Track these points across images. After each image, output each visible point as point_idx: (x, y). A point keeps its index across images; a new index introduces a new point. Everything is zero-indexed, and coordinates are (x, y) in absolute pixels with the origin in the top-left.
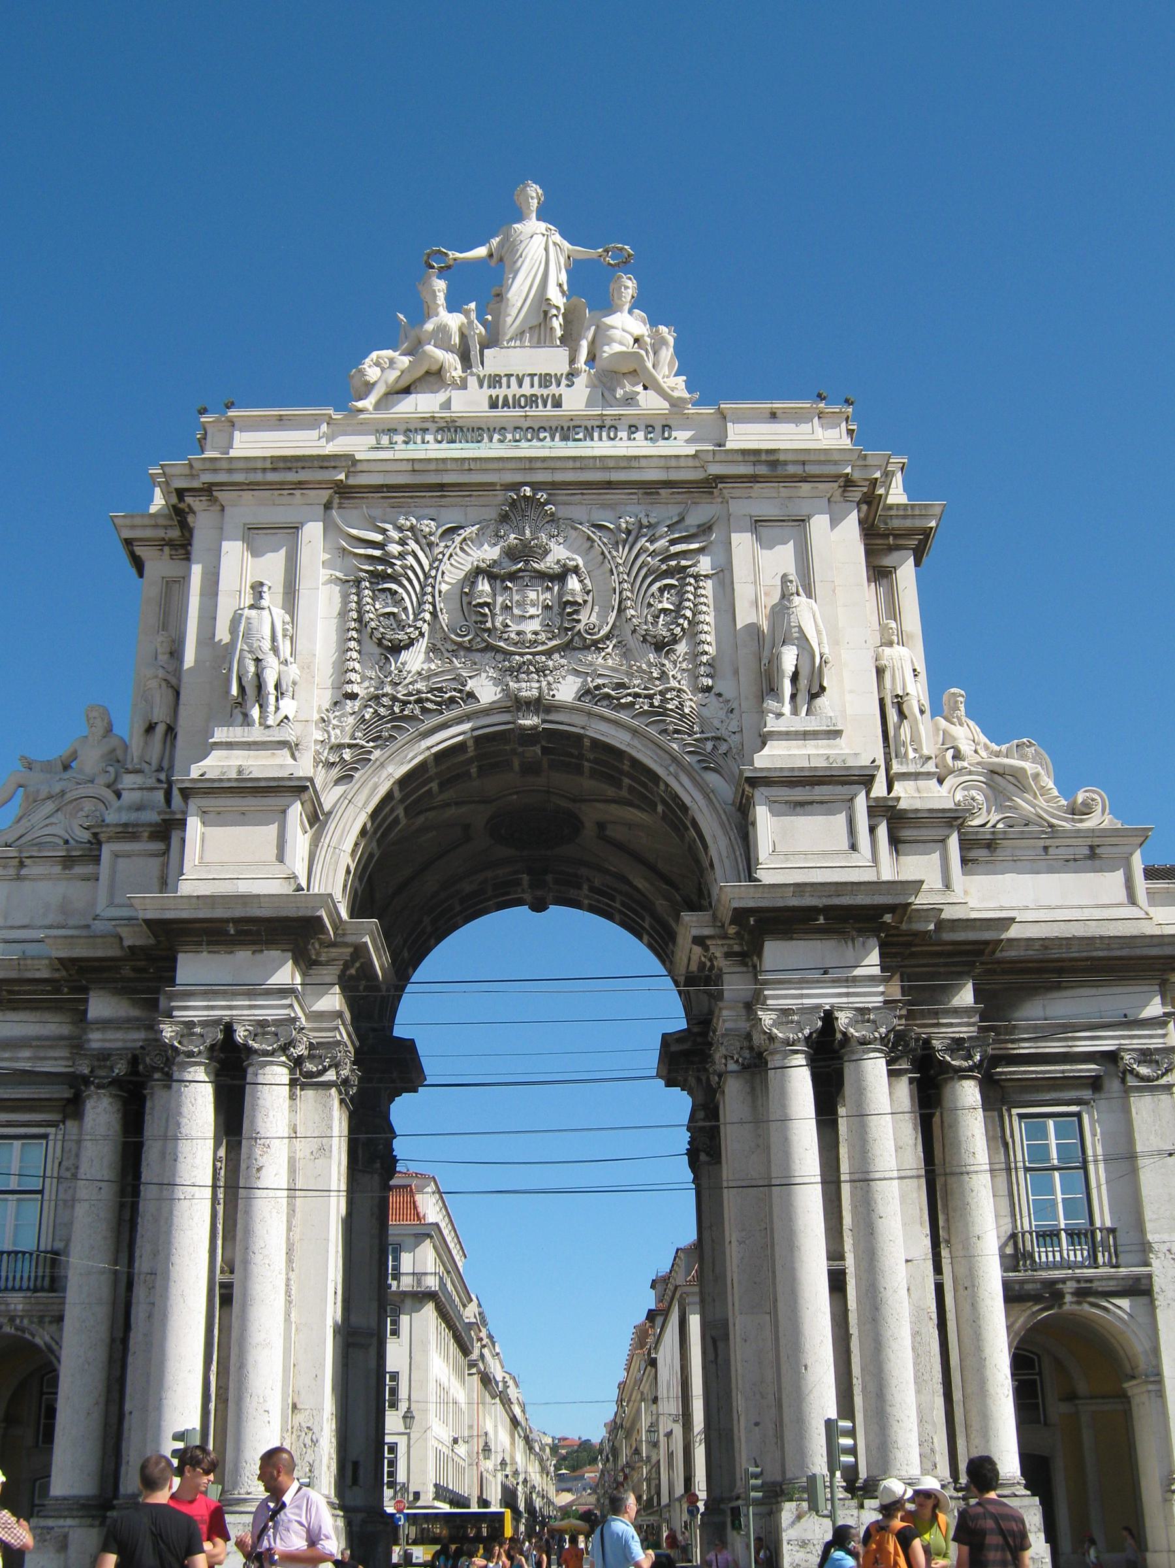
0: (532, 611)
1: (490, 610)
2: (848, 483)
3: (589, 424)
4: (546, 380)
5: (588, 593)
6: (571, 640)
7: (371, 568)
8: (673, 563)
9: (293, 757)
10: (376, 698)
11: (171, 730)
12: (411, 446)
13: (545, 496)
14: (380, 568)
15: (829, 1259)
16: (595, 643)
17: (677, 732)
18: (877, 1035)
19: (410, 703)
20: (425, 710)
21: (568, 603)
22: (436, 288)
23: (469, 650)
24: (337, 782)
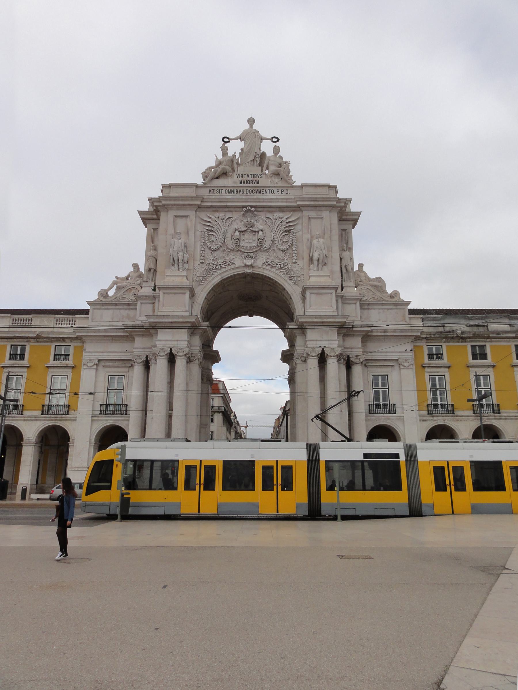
0: (250, 241)
1: (239, 241)
2: (334, 207)
3: (266, 189)
4: (255, 176)
6: (260, 249)
7: (207, 228)
8: (288, 228)
9: (187, 279)
10: (209, 263)
11: (155, 270)
13: (254, 209)
14: (210, 228)
15: (321, 411)
16: (266, 250)
17: (287, 274)
18: (335, 355)
19: (218, 265)
20: (221, 267)
21: (259, 239)
23: (234, 251)
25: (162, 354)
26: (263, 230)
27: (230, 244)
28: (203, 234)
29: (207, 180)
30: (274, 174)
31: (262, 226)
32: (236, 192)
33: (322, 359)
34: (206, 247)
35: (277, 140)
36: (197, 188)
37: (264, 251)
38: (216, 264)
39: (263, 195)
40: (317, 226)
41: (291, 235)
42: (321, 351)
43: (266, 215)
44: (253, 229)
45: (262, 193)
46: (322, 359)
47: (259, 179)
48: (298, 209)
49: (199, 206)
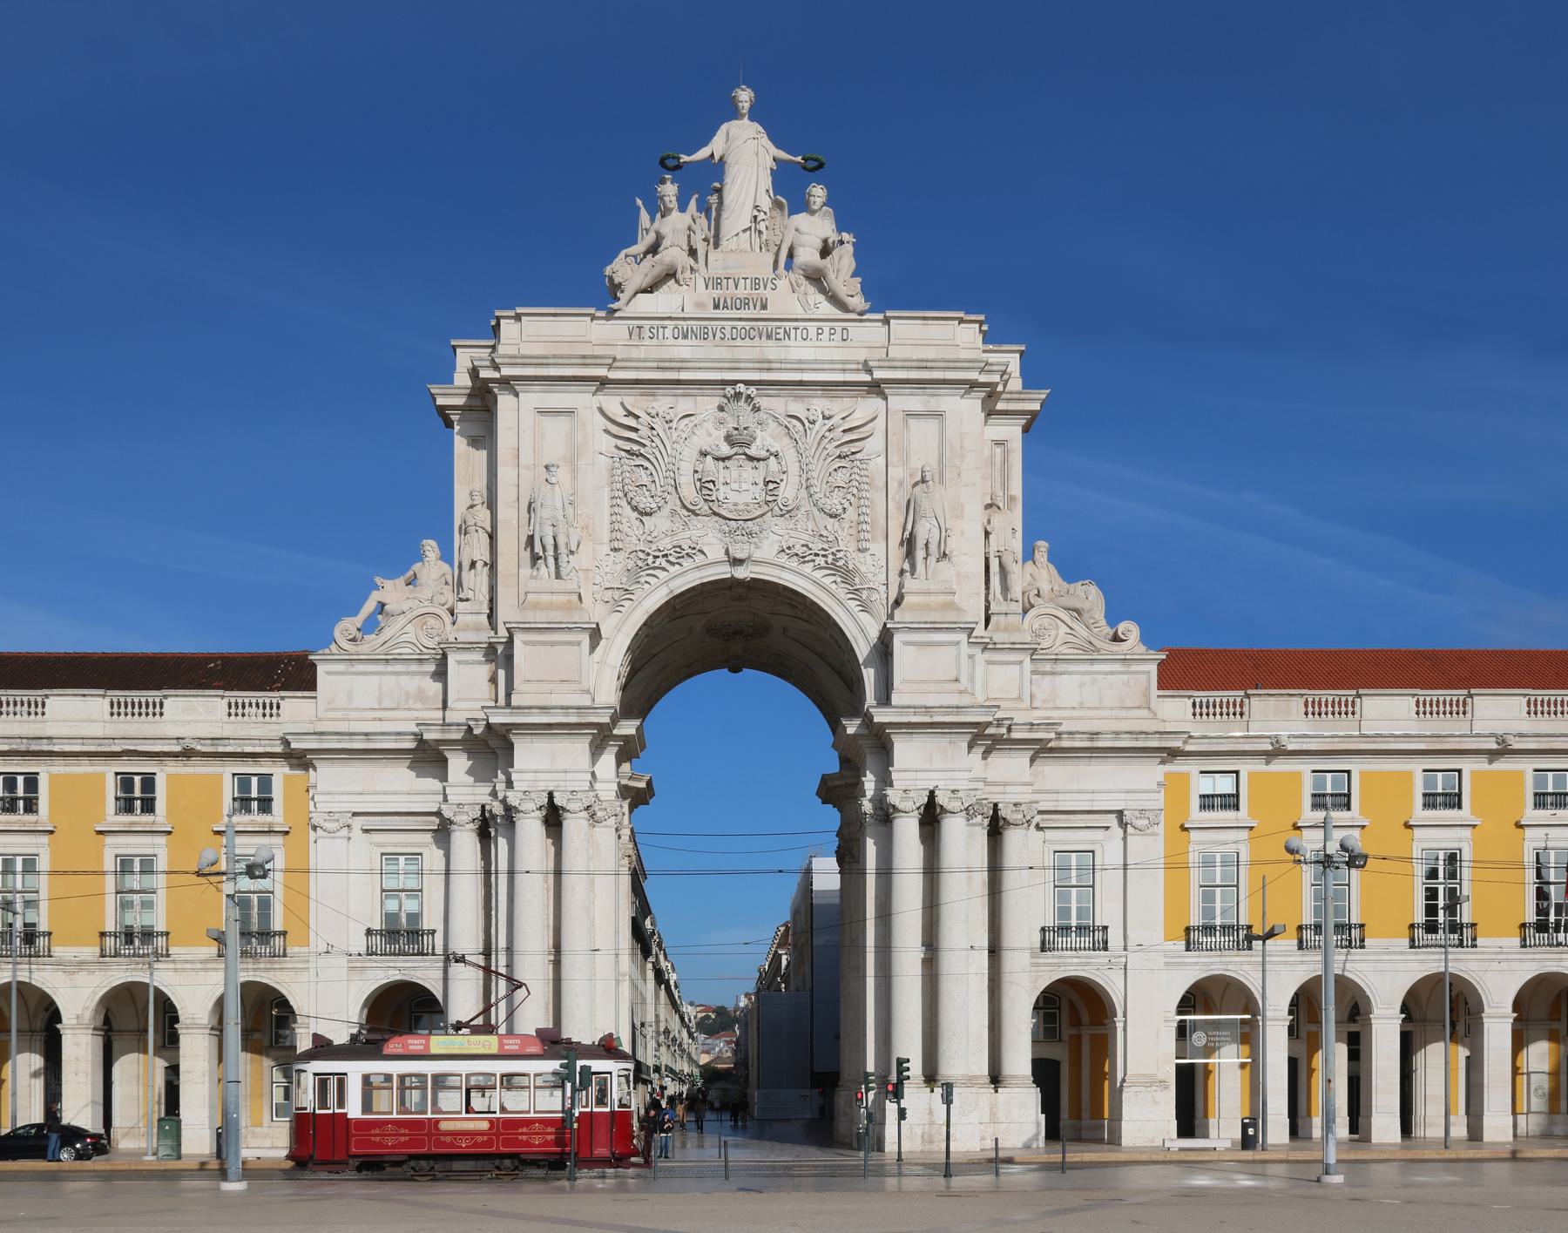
0: (745, 486)
1: (715, 486)
4: (756, 283)
5: (784, 473)
8: (845, 449)
12: (654, 341)
13: (755, 392)
14: (636, 447)
16: (789, 512)
17: (843, 582)
19: (658, 557)
20: (668, 561)
21: (770, 481)
22: (671, 194)
23: (697, 515)
24: (610, 614)
25: (530, 806)
26: (781, 454)
27: (690, 493)
28: (617, 465)
29: (623, 297)
30: (807, 278)
31: (776, 444)
32: (705, 333)
33: (931, 817)
34: (624, 503)
35: (815, 164)
36: (595, 321)
37: (782, 516)
38: (654, 553)
39: (780, 343)
40: (922, 437)
41: (856, 470)
42: (926, 799)
43: (786, 406)
44: (752, 451)
45: (776, 339)
46: (931, 817)
47: (766, 293)
48: (876, 388)
49: (603, 383)
